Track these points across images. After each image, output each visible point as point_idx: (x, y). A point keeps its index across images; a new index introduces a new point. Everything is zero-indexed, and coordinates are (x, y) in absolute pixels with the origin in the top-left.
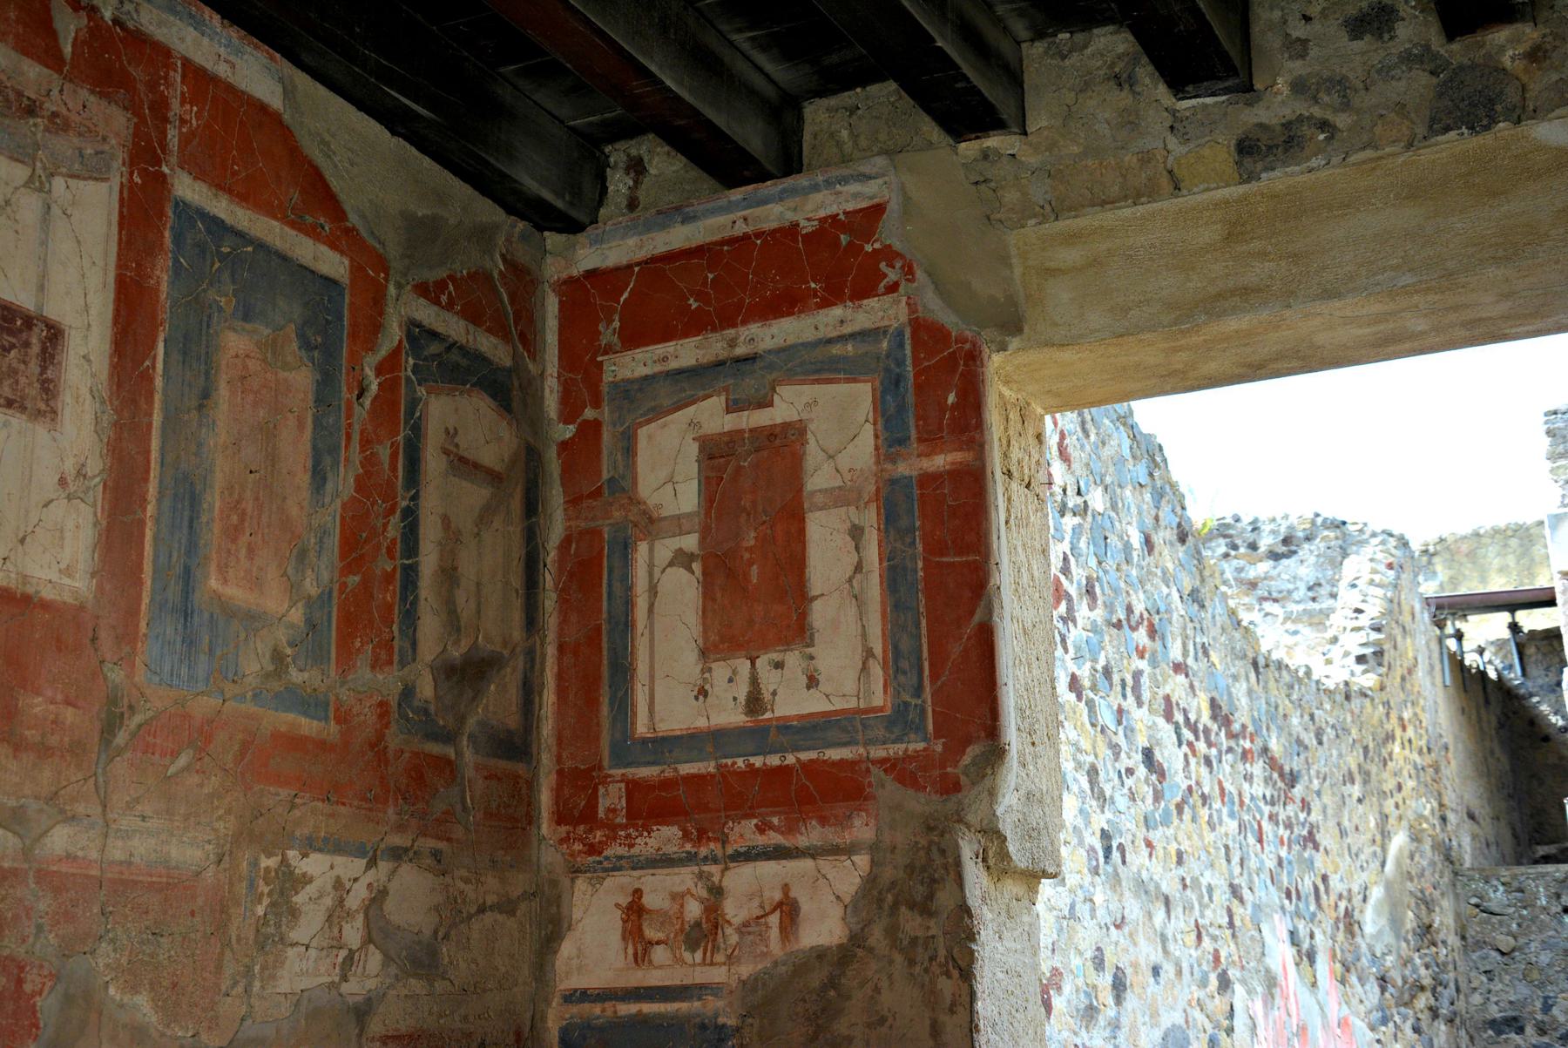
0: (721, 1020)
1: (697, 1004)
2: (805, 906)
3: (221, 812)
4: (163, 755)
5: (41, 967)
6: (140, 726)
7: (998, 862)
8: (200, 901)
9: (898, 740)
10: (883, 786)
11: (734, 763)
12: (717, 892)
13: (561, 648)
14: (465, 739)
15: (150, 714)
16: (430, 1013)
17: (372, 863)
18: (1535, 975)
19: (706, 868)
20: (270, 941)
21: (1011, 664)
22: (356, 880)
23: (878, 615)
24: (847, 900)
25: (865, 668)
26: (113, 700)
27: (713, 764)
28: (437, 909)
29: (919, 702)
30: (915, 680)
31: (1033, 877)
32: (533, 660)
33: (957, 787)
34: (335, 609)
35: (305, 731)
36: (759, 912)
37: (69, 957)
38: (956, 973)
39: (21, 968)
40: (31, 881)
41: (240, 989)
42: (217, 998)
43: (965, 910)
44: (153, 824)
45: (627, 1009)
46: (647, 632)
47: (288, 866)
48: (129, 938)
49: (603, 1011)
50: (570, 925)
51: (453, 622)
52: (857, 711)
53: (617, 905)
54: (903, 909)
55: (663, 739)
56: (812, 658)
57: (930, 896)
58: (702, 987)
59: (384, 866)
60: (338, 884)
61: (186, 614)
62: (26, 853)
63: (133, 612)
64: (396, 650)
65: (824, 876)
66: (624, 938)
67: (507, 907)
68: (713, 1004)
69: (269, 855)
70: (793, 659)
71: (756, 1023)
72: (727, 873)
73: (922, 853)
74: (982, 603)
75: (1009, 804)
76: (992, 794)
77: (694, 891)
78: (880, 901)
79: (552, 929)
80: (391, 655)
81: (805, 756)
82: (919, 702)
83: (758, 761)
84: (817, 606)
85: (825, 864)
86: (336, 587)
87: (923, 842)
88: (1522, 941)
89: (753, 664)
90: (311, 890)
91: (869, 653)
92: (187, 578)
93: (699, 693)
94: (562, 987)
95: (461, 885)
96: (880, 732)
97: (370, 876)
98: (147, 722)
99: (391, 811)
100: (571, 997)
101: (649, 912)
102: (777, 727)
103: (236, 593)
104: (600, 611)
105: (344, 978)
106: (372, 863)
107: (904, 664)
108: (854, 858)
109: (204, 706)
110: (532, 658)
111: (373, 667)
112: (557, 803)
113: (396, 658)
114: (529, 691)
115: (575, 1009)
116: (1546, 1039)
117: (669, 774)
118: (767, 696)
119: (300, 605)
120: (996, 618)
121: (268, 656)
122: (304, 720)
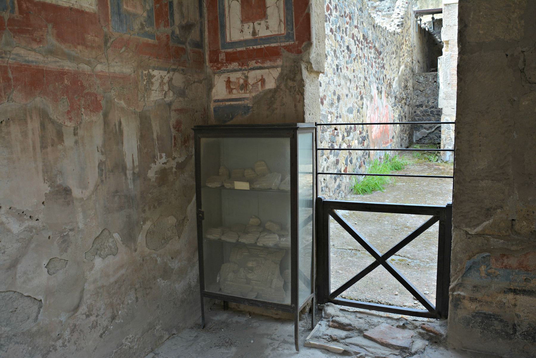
0: (248, 105)
1: (243, 102)
2: (266, 80)
3: (133, 61)
4: (119, 48)
5: (100, 95)
6: (113, 41)
7: (310, 69)
8: (131, 81)
9: (288, 41)
10: (284, 52)
11: (250, 48)
12: (247, 77)
13: (208, 21)
14: (187, 43)
15: (114, 39)
16: (185, 105)
17: (168, 72)
18: (427, 95)
19: (244, 72)
20: (148, 89)
21: (314, 23)
22: (165, 76)
23: (283, 11)
24: (276, 78)
25: (280, 24)
26: (106, 36)
27: (245, 48)
28: (184, 82)
29: (292, 32)
30: (291, 27)
31: (318, 73)
32: (202, 24)
33: (301, 52)
34: (154, 13)
35: (150, 42)
36: (256, 81)
37: (105, 93)
38: (300, 94)
39: (96, 95)
40: (95, 76)
41: (142, 100)
42: (138, 102)
43: (302, 80)
44: (119, 64)
45: (229, 103)
46: (228, 17)
47: (150, 73)
48: (117, 89)
49: (223, 104)
50: (214, 85)
51: (182, 15)
52: (278, 35)
53: (224, 81)
54: (288, 80)
55: (233, 42)
56: (267, 22)
57: (295, 77)
58: (244, 98)
59: (171, 73)
60: (161, 77)
61: (119, 14)
62: (93, 70)
63: (107, 14)
64: (169, 22)
65: (271, 73)
66: (226, 88)
67: (200, 82)
68: (247, 102)
69: (145, 71)
70: (263, 22)
71: (256, 105)
72: (249, 73)
73: (293, 67)
74: (307, 8)
75: (313, 56)
76: (309, 54)
77: (241, 77)
78: (283, 78)
79: (210, 87)
80: (168, 24)
81: (266, 46)
82: (292, 32)
83: (255, 47)
84: (268, 9)
85: (271, 70)
86: (154, 7)
87: (293, 65)
88: (425, 88)
89: (253, 24)
90: (155, 78)
91: (281, 21)
92: (119, 6)
93: (241, 31)
94: (213, 99)
95: (189, 77)
96: (283, 40)
97: (168, 75)
98: (114, 41)
99: (172, 60)
100: (215, 101)
101: (232, 82)
102: (260, 39)
103: (130, 9)
104: (217, 11)
105: (165, 97)
106: (168, 72)
107: (289, 23)
108: (278, 69)
109: (126, 36)
110: (202, 24)
111: (164, 27)
112: (210, 58)
113: (170, 24)
114: (202, 32)
115: (216, 104)
116: (427, 108)
117: (235, 51)
118: (257, 32)
119: (146, 12)
120: (311, 12)
121: (140, 24)
122: (150, 40)
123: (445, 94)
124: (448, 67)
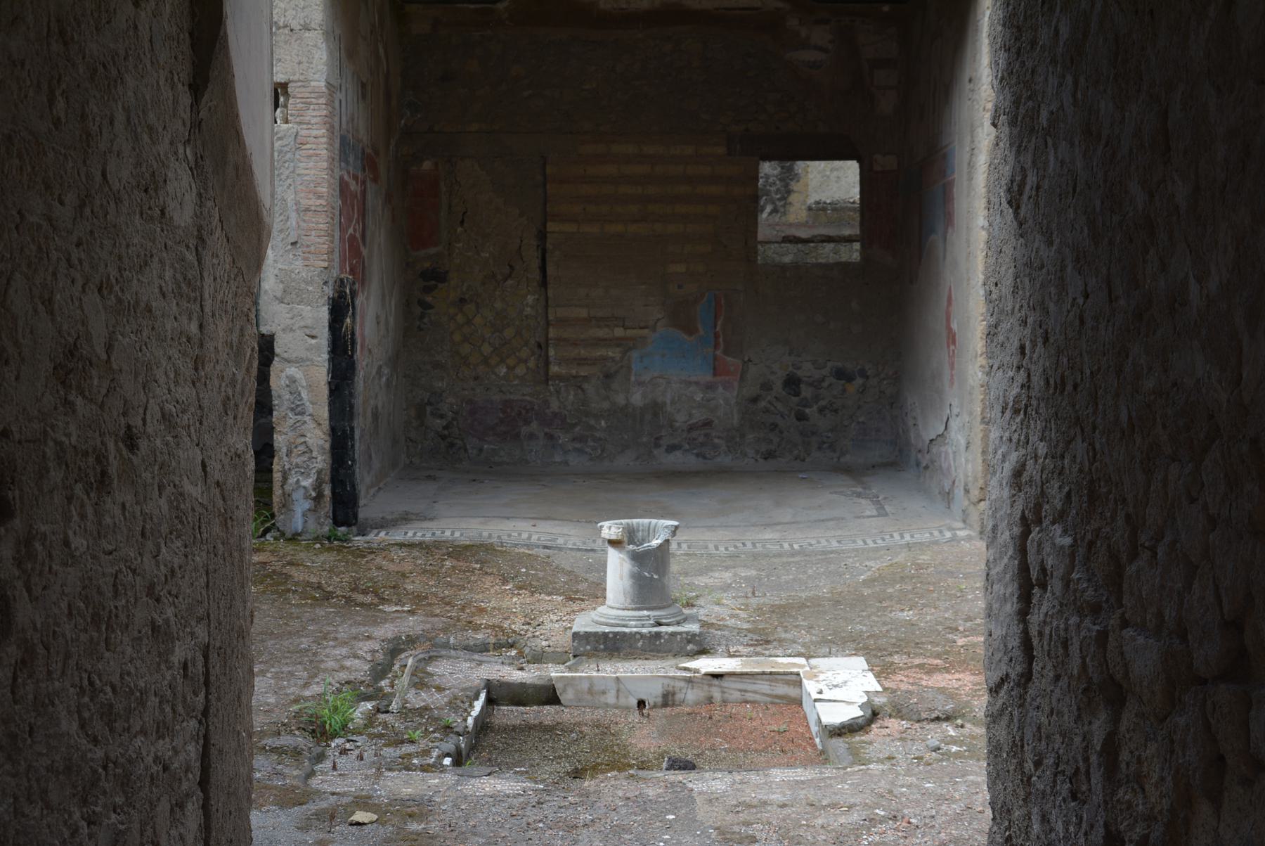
123: (282, 282)
124: (289, 181)
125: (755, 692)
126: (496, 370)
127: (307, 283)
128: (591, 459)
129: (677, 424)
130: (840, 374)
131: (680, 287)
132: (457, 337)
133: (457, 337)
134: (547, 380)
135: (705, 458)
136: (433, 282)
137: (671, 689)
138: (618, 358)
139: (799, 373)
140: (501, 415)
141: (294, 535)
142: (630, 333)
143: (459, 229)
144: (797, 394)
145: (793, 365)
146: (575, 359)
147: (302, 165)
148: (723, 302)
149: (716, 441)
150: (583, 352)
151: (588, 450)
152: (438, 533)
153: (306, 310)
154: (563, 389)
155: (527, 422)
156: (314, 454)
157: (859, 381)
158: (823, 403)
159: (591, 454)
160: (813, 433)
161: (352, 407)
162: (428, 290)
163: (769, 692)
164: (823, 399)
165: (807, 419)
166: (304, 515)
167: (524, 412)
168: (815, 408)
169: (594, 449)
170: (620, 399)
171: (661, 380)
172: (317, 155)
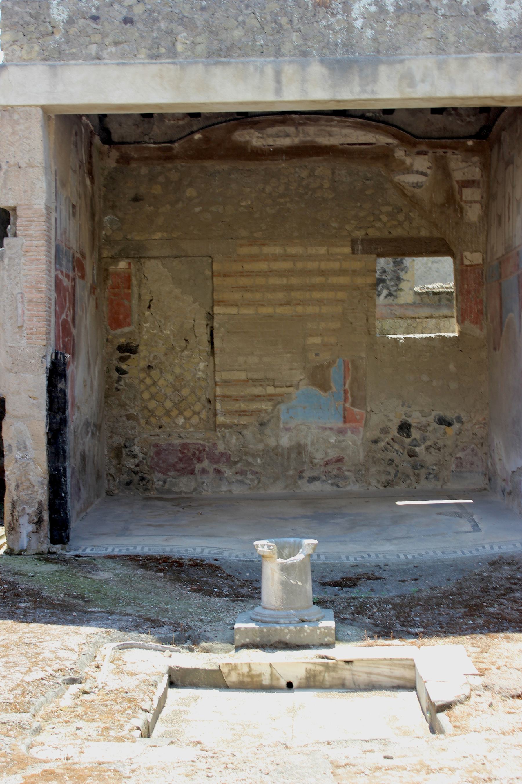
123: (11, 357)
124: (17, 280)
125: (379, 674)
126: (176, 421)
127: (30, 357)
128: (250, 489)
129: (316, 461)
130: (443, 421)
131: (317, 355)
132: (146, 396)
133: (146, 396)
134: (215, 427)
135: (338, 486)
136: (127, 354)
137: (312, 672)
138: (269, 410)
139: (410, 420)
140: (180, 455)
141: (21, 551)
142: (279, 390)
143: (147, 313)
144: (409, 436)
145: (405, 414)
146: (236, 411)
147: (25, 267)
148: (350, 366)
149: (347, 473)
150: (242, 405)
151: (248, 481)
152: (131, 548)
153: (29, 377)
154: (228, 435)
155: (200, 460)
156: (36, 488)
157: (456, 426)
158: (428, 443)
159: (250, 485)
160: (422, 467)
161: (64, 451)
162: (123, 359)
163: (389, 674)
164: (429, 440)
165: (417, 456)
166: (28, 536)
167: (197, 452)
168: (423, 447)
169: (252, 480)
170: (272, 442)
171: (303, 427)
172: (38, 260)
